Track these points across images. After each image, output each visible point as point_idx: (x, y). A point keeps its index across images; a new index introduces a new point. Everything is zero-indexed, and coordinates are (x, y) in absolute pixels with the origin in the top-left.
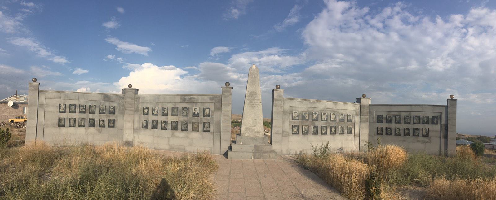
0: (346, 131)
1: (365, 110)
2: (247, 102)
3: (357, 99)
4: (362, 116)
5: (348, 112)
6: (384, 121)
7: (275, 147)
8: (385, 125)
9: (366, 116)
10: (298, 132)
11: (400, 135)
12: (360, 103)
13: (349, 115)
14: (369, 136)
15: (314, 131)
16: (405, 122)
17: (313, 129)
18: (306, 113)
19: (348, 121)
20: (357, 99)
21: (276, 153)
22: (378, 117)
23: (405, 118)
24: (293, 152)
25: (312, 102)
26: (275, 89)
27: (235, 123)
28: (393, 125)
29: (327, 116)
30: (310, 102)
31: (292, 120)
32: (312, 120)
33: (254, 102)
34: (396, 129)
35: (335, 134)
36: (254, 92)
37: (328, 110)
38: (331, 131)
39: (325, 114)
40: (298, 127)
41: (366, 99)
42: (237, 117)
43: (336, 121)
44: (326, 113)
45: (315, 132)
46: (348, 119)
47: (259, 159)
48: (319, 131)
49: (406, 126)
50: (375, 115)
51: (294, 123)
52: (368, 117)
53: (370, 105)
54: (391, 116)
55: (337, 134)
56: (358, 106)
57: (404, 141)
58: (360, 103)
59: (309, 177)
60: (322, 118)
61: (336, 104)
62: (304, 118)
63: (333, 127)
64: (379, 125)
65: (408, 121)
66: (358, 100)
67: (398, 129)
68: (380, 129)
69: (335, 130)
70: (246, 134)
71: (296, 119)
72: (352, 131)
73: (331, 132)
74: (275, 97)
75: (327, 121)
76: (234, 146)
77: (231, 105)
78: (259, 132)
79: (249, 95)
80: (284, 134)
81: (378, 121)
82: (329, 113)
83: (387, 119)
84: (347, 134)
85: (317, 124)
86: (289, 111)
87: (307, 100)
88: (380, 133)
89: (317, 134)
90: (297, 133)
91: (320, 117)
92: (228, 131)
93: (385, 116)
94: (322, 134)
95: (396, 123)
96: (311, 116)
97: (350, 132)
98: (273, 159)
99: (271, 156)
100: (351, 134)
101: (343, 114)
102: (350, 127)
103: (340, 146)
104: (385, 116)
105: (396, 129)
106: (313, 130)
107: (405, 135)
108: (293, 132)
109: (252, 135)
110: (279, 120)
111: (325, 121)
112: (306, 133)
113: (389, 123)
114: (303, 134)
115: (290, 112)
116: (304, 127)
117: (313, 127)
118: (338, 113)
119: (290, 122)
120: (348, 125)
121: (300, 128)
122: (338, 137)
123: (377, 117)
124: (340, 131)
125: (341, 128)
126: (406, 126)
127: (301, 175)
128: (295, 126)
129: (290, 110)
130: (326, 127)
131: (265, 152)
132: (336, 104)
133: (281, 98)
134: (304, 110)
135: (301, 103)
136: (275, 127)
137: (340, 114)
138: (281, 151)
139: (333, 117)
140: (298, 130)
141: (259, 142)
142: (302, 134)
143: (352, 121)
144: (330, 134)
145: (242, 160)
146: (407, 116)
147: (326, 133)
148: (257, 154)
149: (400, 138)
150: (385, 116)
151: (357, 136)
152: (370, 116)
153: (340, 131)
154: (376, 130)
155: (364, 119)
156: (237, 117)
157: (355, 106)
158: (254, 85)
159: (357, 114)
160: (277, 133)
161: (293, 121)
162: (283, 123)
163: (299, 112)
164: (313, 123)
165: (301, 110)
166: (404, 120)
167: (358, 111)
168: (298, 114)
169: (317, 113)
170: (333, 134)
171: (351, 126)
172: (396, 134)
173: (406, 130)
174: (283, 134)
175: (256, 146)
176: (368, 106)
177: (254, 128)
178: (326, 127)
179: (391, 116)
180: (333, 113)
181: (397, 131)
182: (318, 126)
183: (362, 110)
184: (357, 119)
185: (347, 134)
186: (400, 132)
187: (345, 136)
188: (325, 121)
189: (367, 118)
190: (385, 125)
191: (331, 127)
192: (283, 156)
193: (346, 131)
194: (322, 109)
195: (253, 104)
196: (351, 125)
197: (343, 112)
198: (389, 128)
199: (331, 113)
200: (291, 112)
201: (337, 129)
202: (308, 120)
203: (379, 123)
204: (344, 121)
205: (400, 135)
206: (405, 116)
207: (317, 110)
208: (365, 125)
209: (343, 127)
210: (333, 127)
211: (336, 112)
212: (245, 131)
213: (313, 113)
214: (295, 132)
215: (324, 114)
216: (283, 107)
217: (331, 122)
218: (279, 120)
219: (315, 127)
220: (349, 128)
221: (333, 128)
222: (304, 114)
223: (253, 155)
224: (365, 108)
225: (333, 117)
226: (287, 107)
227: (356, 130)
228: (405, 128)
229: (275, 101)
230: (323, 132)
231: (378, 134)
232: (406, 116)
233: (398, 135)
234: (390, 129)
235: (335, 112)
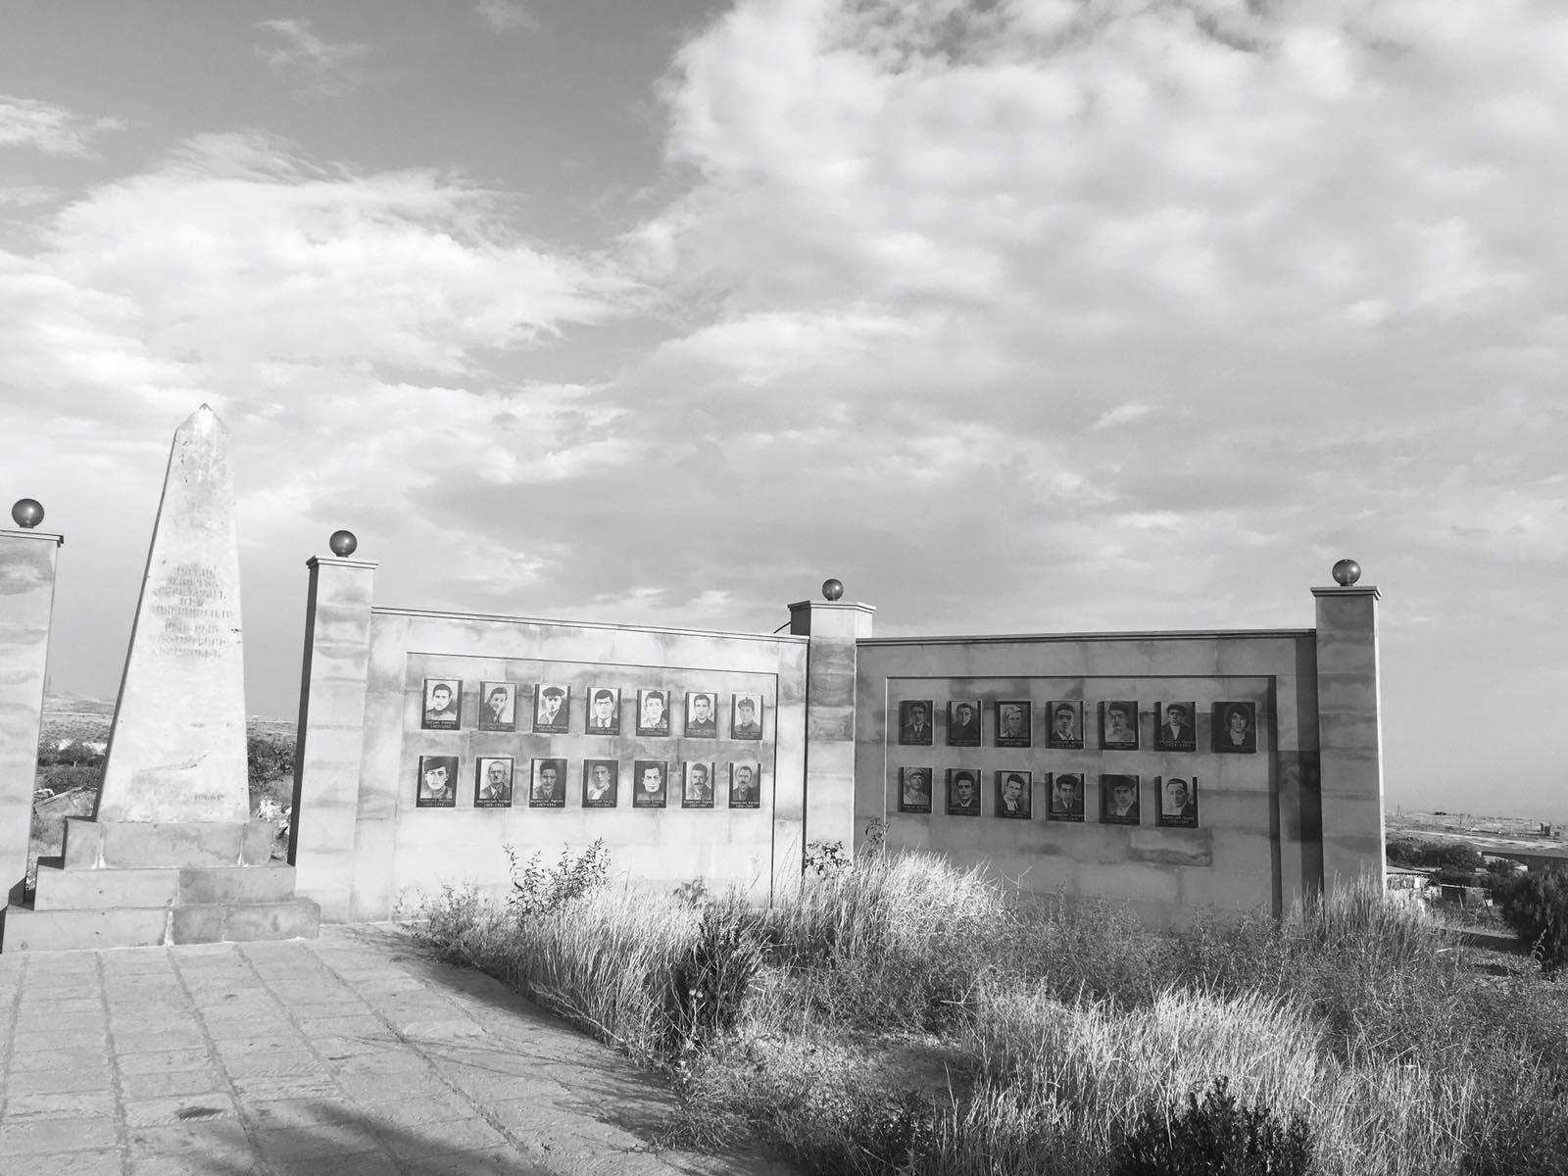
0: (722, 791)
1: (837, 672)
2: (150, 624)
3: (792, 608)
4: (822, 704)
5: (741, 689)
6: (939, 732)
7: (310, 875)
8: (940, 758)
9: (838, 705)
10: (449, 796)
11: (1028, 816)
12: (808, 633)
13: (742, 704)
14: (856, 818)
15: (541, 790)
16: (1053, 741)
17: (536, 775)
18: (500, 691)
19: (734, 736)
20: (792, 608)
21: (317, 907)
22: (907, 709)
23: (1051, 713)
24: (413, 904)
25: (537, 629)
26: (325, 553)
27: (60, 768)
28: (988, 759)
29: (619, 707)
30: (523, 633)
31: (419, 730)
32: (535, 730)
33: (192, 626)
34: (1005, 777)
35: (663, 805)
36: (194, 568)
37: (623, 675)
38: (638, 787)
39: (610, 694)
40: (452, 767)
41: (838, 607)
42: (77, 717)
43: (667, 733)
44: (615, 693)
45: (548, 791)
46: (738, 722)
47: (209, 940)
48: (573, 790)
49: (1058, 762)
50: (887, 697)
51: (433, 743)
52: (847, 710)
53: (862, 644)
54: (975, 705)
55: (673, 808)
56: (793, 651)
57: (1050, 850)
58: (809, 634)
59: (461, 990)
60: (592, 717)
61: (667, 637)
62: (487, 716)
63: (652, 765)
64: (913, 758)
65: (1070, 733)
66: (800, 617)
67: (1015, 777)
68: (914, 781)
69: (663, 787)
70: (137, 813)
71: (441, 725)
72: (758, 788)
73: (640, 797)
74: (322, 600)
75: (617, 733)
76: (47, 884)
77: (43, 645)
78: (220, 797)
79: (164, 583)
80: (367, 802)
81: (908, 735)
82: (629, 693)
83: (955, 719)
84: (731, 806)
85: (559, 748)
86: (403, 678)
87: (506, 620)
88: (916, 802)
89: (561, 805)
90: (444, 800)
91: (577, 710)
92: (14, 799)
93: (939, 706)
94: (587, 803)
95: (1000, 743)
96: (526, 705)
97: (748, 798)
98: (298, 938)
99: (286, 921)
100: (757, 806)
101: (712, 698)
102: (746, 768)
103: (689, 876)
104: (939, 706)
105: (1005, 777)
106: (537, 784)
107: (1052, 816)
108: (425, 795)
109: (169, 815)
110: (341, 727)
111: (604, 731)
112: (499, 798)
113: (962, 745)
114: (479, 804)
115: (407, 685)
116: (485, 764)
117: (538, 764)
118: (680, 688)
119: (406, 736)
120: (738, 759)
121: (464, 772)
122: (676, 820)
123: (897, 708)
124: (692, 790)
125: (699, 773)
126: (1058, 762)
127: (423, 986)
128: (436, 763)
129: (408, 672)
130: (613, 767)
131: (246, 904)
132: (667, 637)
133: (359, 608)
134: (491, 672)
135: (475, 637)
136: (320, 765)
137: (692, 697)
138: (348, 898)
139: (652, 713)
140: (451, 783)
141: (214, 853)
142: (477, 805)
143: (759, 736)
144: (636, 804)
145: (101, 952)
146: (1065, 706)
147: (610, 800)
148: (197, 918)
149: (1028, 833)
150: (943, 707)
151: (787, 818)
152: (860, 705)
153: (692, 790)
154: (896, 783)
155: (831, 725)
156: (77, 717)
157: (773, 651)
158: (202, 526)
159: (788, 696)
160: (324, 803)
161: (426, 731)
162: (368, 744)
163: (460, 683)
164: (540, 745)
165: (471, 674)
166: (1043, 729)
167: (796, 677)
168: (455, 696)
169: (565, 689)
170: (649, 805)
171: (753, 765)
172: (1001, 812)
173: (1060, 787)
174: (366, 806)
175: (190, 877)
176: (848, 650)
177: (186, 774)
178: (613, 767)
179: (975, 705)
180: (652, 688)
181: (1011, 791)
182: (565, 762)
183: (819, 670)
184: (791, 720)
185: (731, 806)
186: (1026, 795)
187: (721, 815)
188: (604, 731)
189: (848, 720)
190: (940, 758)
191: (640, 769)
192: (358, 926)
193: (722, 791)
194: (588, 667)
195: (188, 640)
196: (754, 756)
197: (710, 685)
198: (964, 775)
199: (639, 693)
200: (419, 685)
201: (675, 777)
202: (510, 728)
203: (908, 743)
204: (714, 736)
205: (1023, 813)
206: (1049, 704)
207: (561, 677)
208: (837, 763)
209: (709, 766)
210: (652, 765)
211: (669, 682)
212: (131, 790)
213: (542, 688)
214: (432, 792)
215: (601, 695)
216: (370, 659)
217: (641, 740)
218: (341, 727)
219: (548, 764)
220: (743, 772)
221: (649, 772)
222: (487, 695)
223: (170, 922)
224: (832, 660)
225: (652, 713)
226: (392, 653)
227: (784, 785)
228: (1055, 777)
229: (325, 621)
230: (596, 795)
231: (903, 808)
232: (1055, 706)
233: (1013, 815)
234: (972, 780)
235: (661, 685)
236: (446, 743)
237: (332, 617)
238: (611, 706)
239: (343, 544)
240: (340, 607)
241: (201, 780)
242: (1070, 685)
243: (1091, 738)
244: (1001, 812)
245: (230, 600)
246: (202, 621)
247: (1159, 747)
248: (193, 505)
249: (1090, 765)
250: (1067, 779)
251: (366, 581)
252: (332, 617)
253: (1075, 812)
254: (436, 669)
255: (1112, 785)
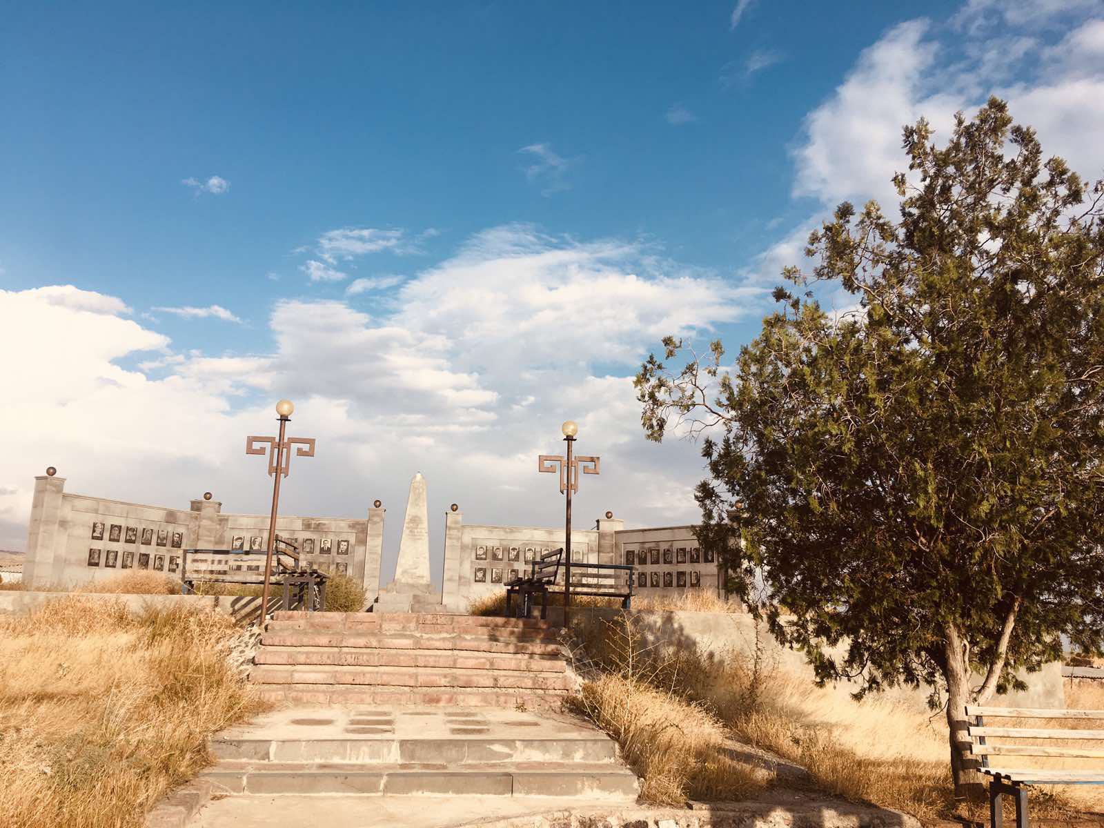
16: (665, 562)
40: (485, 571)
62: (495, 557)
67: (655, 574)
71: (481, 559)
90: (483, 581)
95: (652, 563)
116: (494, 570)
119: (472, 562)
128: (480, 569)
133: (458, 525)
134: (496, 544)
140: (484, 575)
146: (668, 550)
149: (659, 591)
162: (461, 564)
164: (511, 565)
165: (490, 544)
172: (652, 585)
181: (655, 578)
200: (475, 547)
202: (501, 560)
215: (529, 550)
219: (513, 571)
226: (467, 538)
236: (483, 564)
237: (450, 528)
238: (532, 554)
239: (454, 508)
240: (453, 525)
241: (419, 572)
242: (670, 543)
243: (674, 560)
244: (652, 585)
245: (425, 525)
246: (419, 530)
247: (692, 562)
248: (416, 500)
249: (674, 569)
250: (669, 573)
251: (460, 518)
252: (450, 528)
253: (670, 584)
254: (480, 543)
255: (681, 574)
